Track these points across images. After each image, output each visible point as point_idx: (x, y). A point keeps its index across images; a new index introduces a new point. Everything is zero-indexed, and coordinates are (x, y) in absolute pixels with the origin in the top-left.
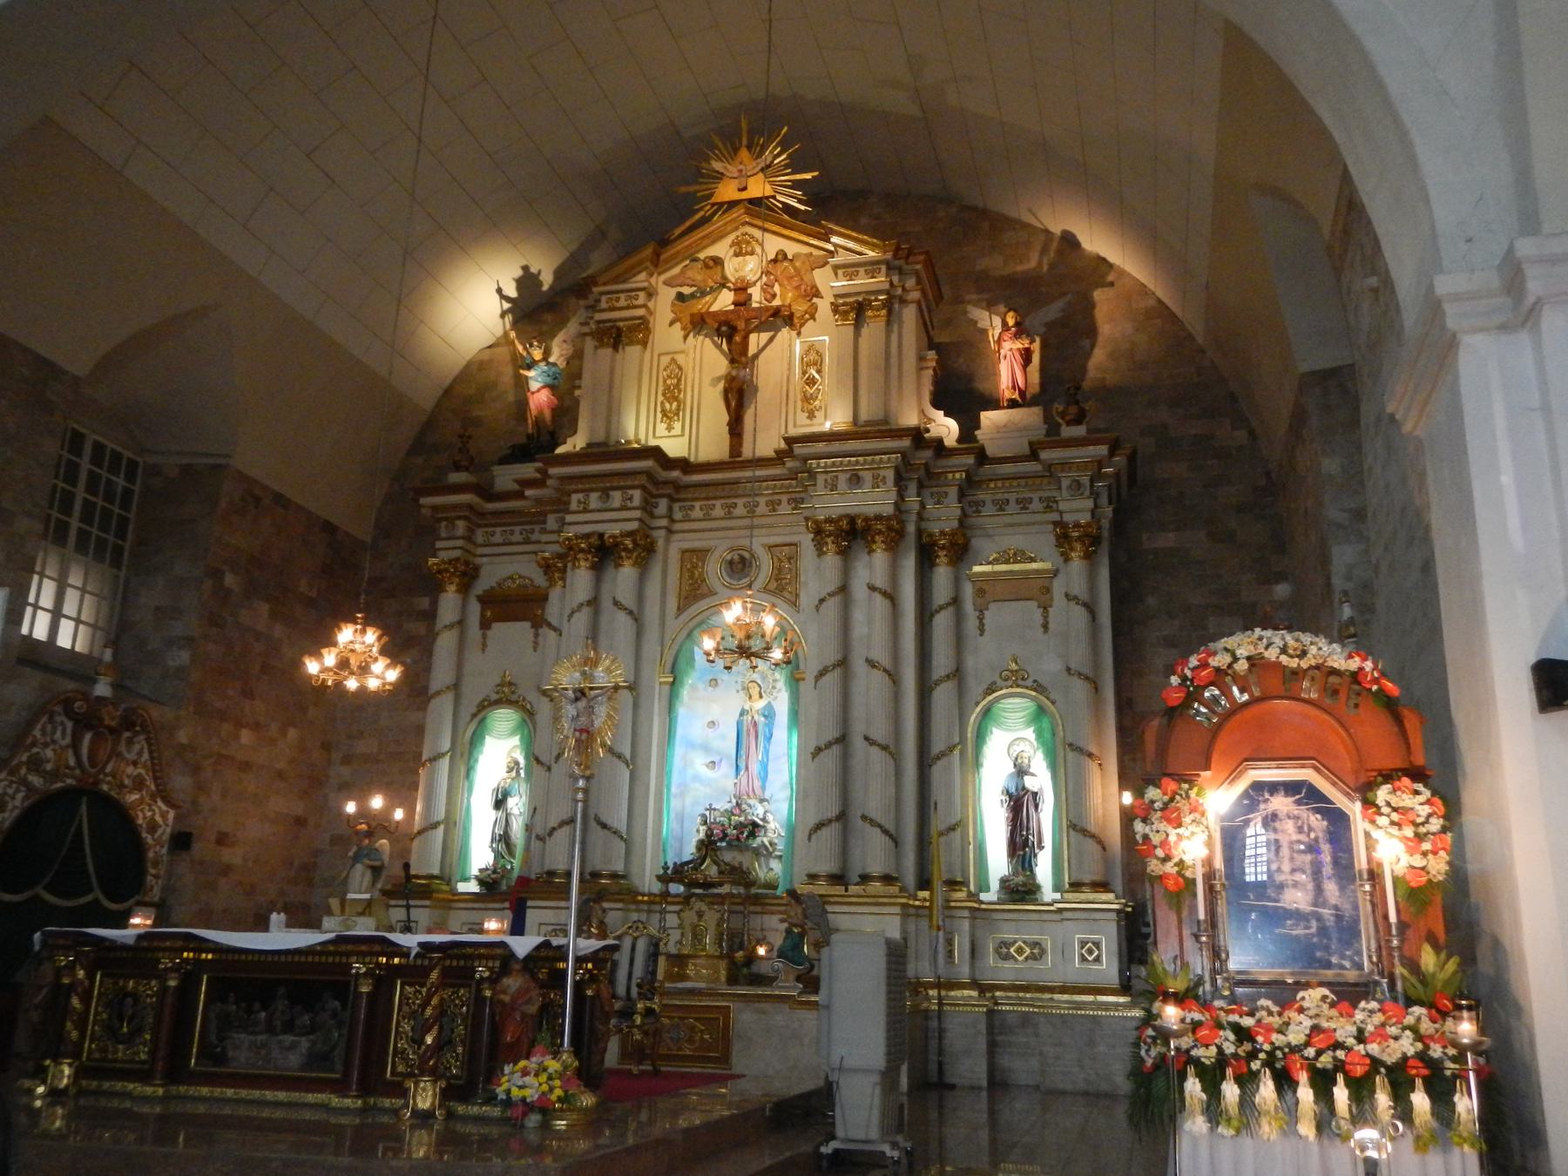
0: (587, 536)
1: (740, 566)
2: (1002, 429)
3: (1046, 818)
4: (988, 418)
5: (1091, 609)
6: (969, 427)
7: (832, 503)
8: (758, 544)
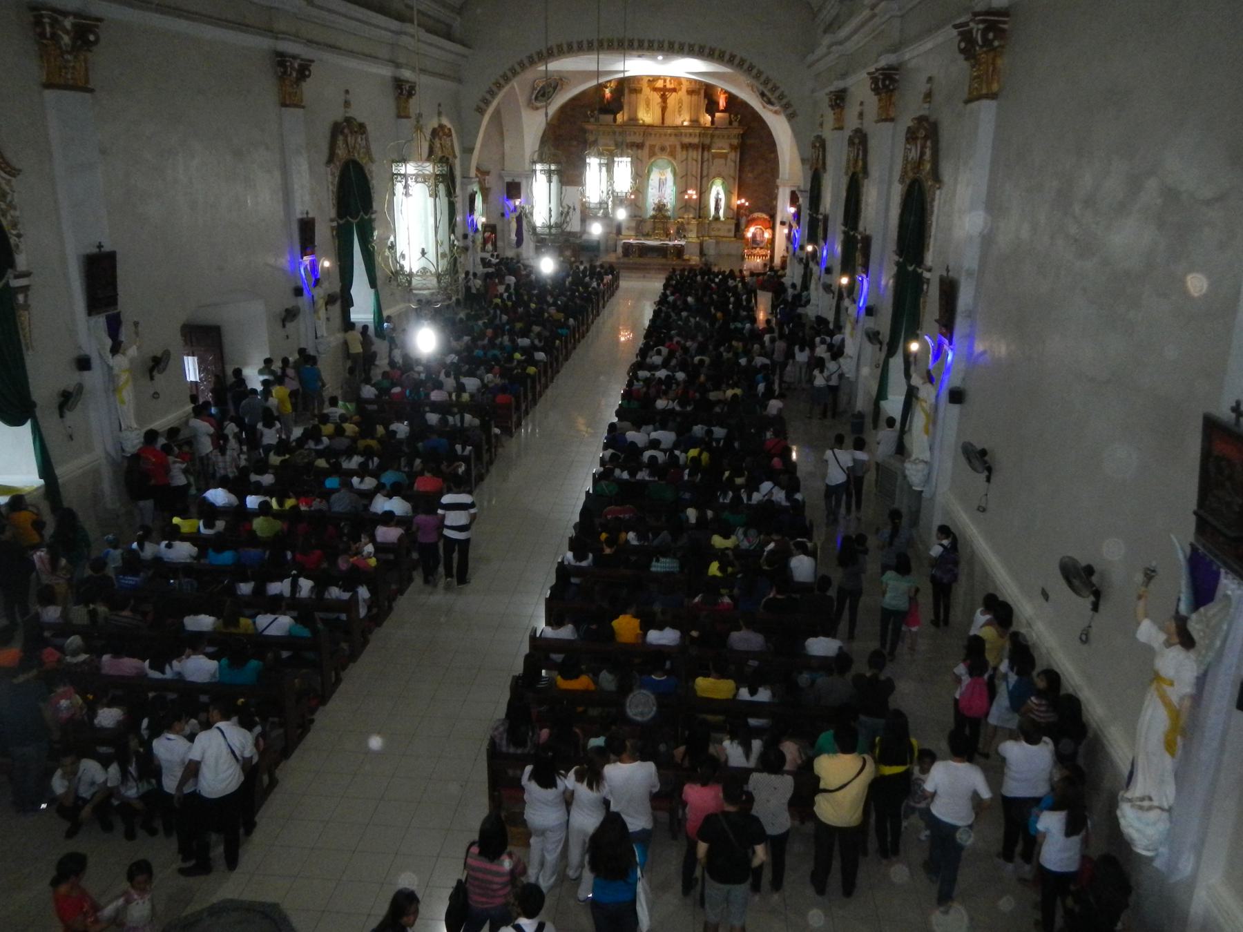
0: (631, 143)
1: (663, 149)
2: (720, 118)
3: (722, 204)
4: (717, 115)
5: (735, 162)
6: (713, 117)
7: (686, 140)
8: (667, 144)
